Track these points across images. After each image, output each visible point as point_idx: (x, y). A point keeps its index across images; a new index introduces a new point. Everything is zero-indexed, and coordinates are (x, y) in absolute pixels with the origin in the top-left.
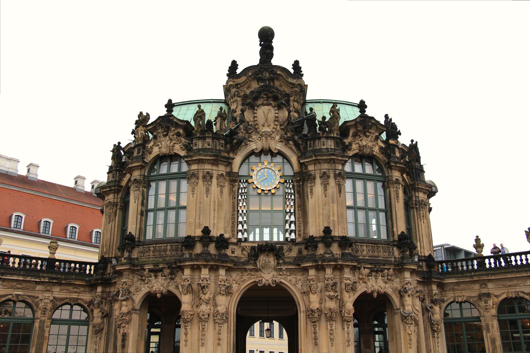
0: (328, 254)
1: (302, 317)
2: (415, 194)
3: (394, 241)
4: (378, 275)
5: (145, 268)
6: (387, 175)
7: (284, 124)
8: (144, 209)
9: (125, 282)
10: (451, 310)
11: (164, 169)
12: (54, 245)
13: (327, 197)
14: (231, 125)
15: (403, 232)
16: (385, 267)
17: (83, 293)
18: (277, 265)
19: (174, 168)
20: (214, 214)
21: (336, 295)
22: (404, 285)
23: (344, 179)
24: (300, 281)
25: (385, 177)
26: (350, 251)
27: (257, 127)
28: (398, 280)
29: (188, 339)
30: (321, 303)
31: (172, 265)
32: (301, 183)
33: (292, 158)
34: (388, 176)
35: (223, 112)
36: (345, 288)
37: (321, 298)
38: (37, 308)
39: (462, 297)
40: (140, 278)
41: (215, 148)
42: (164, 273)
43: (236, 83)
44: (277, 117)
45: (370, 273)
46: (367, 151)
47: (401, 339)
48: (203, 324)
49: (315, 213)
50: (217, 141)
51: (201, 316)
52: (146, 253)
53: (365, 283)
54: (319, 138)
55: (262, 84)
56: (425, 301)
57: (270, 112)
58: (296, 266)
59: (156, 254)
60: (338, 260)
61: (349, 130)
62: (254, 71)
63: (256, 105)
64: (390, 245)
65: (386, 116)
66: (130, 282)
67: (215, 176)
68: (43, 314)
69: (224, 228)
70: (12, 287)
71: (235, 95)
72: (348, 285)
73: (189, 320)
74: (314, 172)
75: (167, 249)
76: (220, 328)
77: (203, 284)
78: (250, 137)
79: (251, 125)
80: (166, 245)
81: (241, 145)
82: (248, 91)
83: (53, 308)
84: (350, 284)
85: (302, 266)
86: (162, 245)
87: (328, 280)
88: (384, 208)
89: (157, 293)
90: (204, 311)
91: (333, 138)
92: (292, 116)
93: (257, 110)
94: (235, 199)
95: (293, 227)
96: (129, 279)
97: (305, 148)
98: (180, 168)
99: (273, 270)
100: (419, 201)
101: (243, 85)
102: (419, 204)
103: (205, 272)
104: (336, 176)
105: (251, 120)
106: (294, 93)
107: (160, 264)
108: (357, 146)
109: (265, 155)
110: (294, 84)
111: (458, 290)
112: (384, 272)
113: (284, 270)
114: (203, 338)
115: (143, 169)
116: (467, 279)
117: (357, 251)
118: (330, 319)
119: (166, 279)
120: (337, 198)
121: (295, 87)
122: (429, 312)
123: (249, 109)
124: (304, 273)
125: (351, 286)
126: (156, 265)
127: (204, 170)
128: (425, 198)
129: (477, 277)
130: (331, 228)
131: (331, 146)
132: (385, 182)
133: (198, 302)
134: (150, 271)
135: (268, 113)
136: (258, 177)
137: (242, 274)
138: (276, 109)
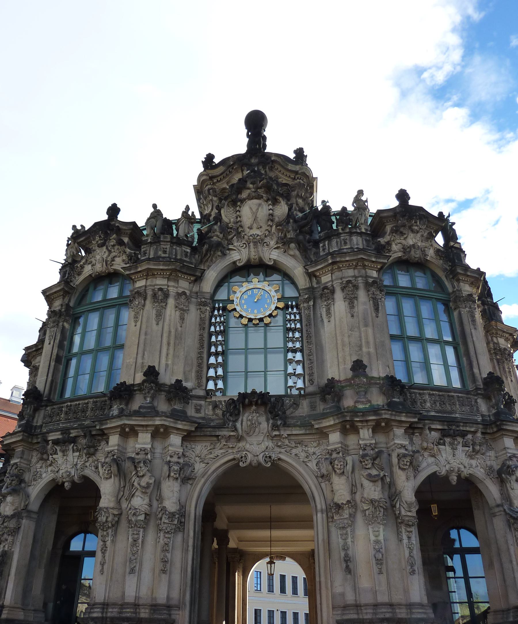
0: (362, 403)
3: (477, 389)
13: (355, 317)
15: (490, 374)
16: (468, 429)
18: (272, 429)
19: (114, 292)
20: (168, 349)
22: (506, 460)
23: (383, 293)
24: (315, 456)
26: (402, 400)
28: (492, 453)
29: (107, 561)
30: (353, 493)
31: (90, 431)
32: (311, 303)
41: (174, 257)
42: (77, 446)
43: (210, 175)
44: (272, 215)
45: (440, 439)
46: (416, 255)
47: (511, 562)
49: (337, 343)
50: (178, 248)
53: (433, 456)
54: (337, 234)
55: (248, 172)
57: (260, 208)
58: (306, 430)
59: (70, 417)
61: (385, 226)
64: (471, 394)
69: (184, 373)
75: (87, 407)
77: (138, 459)
78: (229, 244)
79: (231, 228)
80: (86, 401)
85: (316, 426)
86: (81, 402)
87: (365, 449)
90: (136, 507)
91: (361, 234)
93: (240, 207)
95: (299, 370)
97: (317, 254)
98: (121, 291)
99: (266, 439)
101: (221, 179)
104: (368, 285)
105: (232, 220)
107: (72, 431)
110: (296, 173)
112: (466, 437)
113: (286, 438)
114: (133, 558)
117: (414, 402)
120: (372, 319)
123: (228, 206)
127: (155, 287)
130: (365, 362)
131: (357, 244)
133: (128, 492)
135: (258, 209)
136: (243, 301)
137: (212, 446)
138: (270, 203)
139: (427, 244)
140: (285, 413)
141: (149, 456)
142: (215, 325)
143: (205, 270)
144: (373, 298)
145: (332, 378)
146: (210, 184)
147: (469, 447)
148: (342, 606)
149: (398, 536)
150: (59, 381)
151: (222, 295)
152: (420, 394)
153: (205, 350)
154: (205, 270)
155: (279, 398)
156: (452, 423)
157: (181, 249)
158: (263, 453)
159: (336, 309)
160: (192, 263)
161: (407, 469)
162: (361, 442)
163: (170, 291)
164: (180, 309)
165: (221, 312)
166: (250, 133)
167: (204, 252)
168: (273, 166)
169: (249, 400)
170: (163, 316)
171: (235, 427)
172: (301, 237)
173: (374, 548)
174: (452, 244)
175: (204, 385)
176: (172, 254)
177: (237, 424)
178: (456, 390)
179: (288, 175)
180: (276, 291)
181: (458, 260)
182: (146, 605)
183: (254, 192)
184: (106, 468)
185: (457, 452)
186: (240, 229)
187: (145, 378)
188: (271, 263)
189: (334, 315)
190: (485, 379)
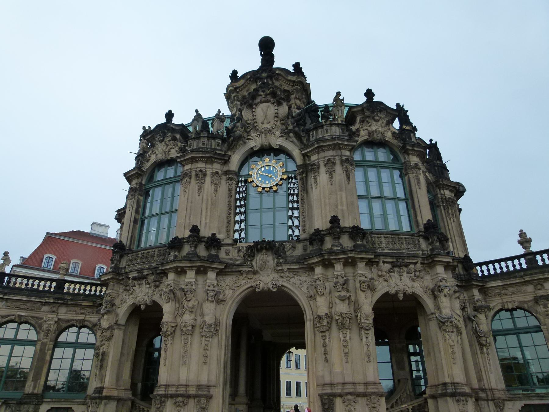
0: (336, 246)
1: (309, 326)
2: (440, 192)
3: (420, 232)
4: (402, 271)
5: (130, 276)
6: (403, 161)
8: (139, 217)
9: (109, 293)
10: (500, 319)
11: (160, 176)
12: (64, 266)
15: (429, 220)
16: (411, 261)
17: (91, 314)
18: (277, 265)
19: (170, 172)
20: (206, 212)
21: (348, 295)
22: (438, 282)
23: (353, 166)
24: (305, 284)
25: (402, 164)
26: (365, 243)
27: (256, 124)
28: (428, 277)
31: (156, 271)
32: (304, 175)
34: (405, 162)
36: (360, 287)
37: (331, 302)
38: (40, 329)
39: (513, 303)
40: (124, 287)
41: (210, 147)
42: (147, 281)
43: (234, 87)
44: (277, 113)
45: (391, 269)
46: (377, 137)
47: (440, 352)
48: (186, 338)
50: (213, 141)
51: (182, 327)
52: (134, 261)
53: (386, 281)
54: (322, 126)
56: (466, 309)
58: (300, 265)
60: (349, 252)
64: (415, 236)
65: (398, 105)
66: (116, 293)
67: (209, 173)
68: (45, 336)
69: (218, 228)
70: (16, 308)
71: (234, 100)
72: (364, 282)
73: (169, 333)
74: (317, 161)
76: (206, 343)
77: (187, 289)
78: (248, 135)
79: (249, 124)
80: (154, 250)
81: (239, 144)
83: (58, 330)
84: (366, 281)
86: (150, 251)
87: (337, 278)
88: (404, 197)
89: (140, 304)
90: (186, 321)
91: (338, 125)
93: (255, 109)
94: (231, 197)
96: (113, 289)
97: (308, 140)
98: (176, 172)
99: (273, 272)
100: (446, 199)
101: (242, 89)
102: (447, 202)
103: (191, 275)
104: (342, 162)
105: (250, 118)
107: (144, 271)
108: (366, 132)
111: (506, 294)
112: (409, 267)
113: (286, 271)
114: (184, 355)
115: (140, 178)
116: (516, 280)
117: (374, 243)
118: (342, 326)
119: (150, 288)
122: (472, 323)
123: (247, 108)
124: (310, 273)
125: (368, 283)
126: (140, 272)
128: (452, 197)
129: (529, 276)
130: (339, 218)
131: (335, 132)
132: (403, 169)
133: (181, 311)
134: (134, 279)
135: (267, 109)
136: (259, 175)
138: (275, 104)
139: (386, 129)
140: (286, 254)
141: (194, 287)
142: (239, 193)
143: (231, 155)
144: (346, 171)
145: (317, 229)
147: (412, 273)
148: (322, 384)
149: (360, 337)
150: (137, 235)
151: (244, 171)
152: (378, 237)
153: (232, 212)
154: (231, 155)
155: (282, 243)
156: (400, 257)
158: (271, 282)
159: (320, 179)
161: (366, 291)
162: (335, 273)
163: (207, 171)
164: (214, 184)
165: (243, 184)
166: (262, 53)
167: (231, 142)
169: (260, 246)
170: (203, 189)
171: (252, 264)
172: (297, 129)
173: (343, 345)
174: (404, 127)
175: (232, 236)
176: (208, 145)
177: (253, 262)
178: (404, 234)
179: (289, 83)
180: (281, 167)
181: (409, 139)
182: (193, 386)
183: (265, 97)
184: (166, 295)
185: (402, 278)
187: (191, 233)
188: (277, 147)
189: (320, 184)
190: (425, 225)
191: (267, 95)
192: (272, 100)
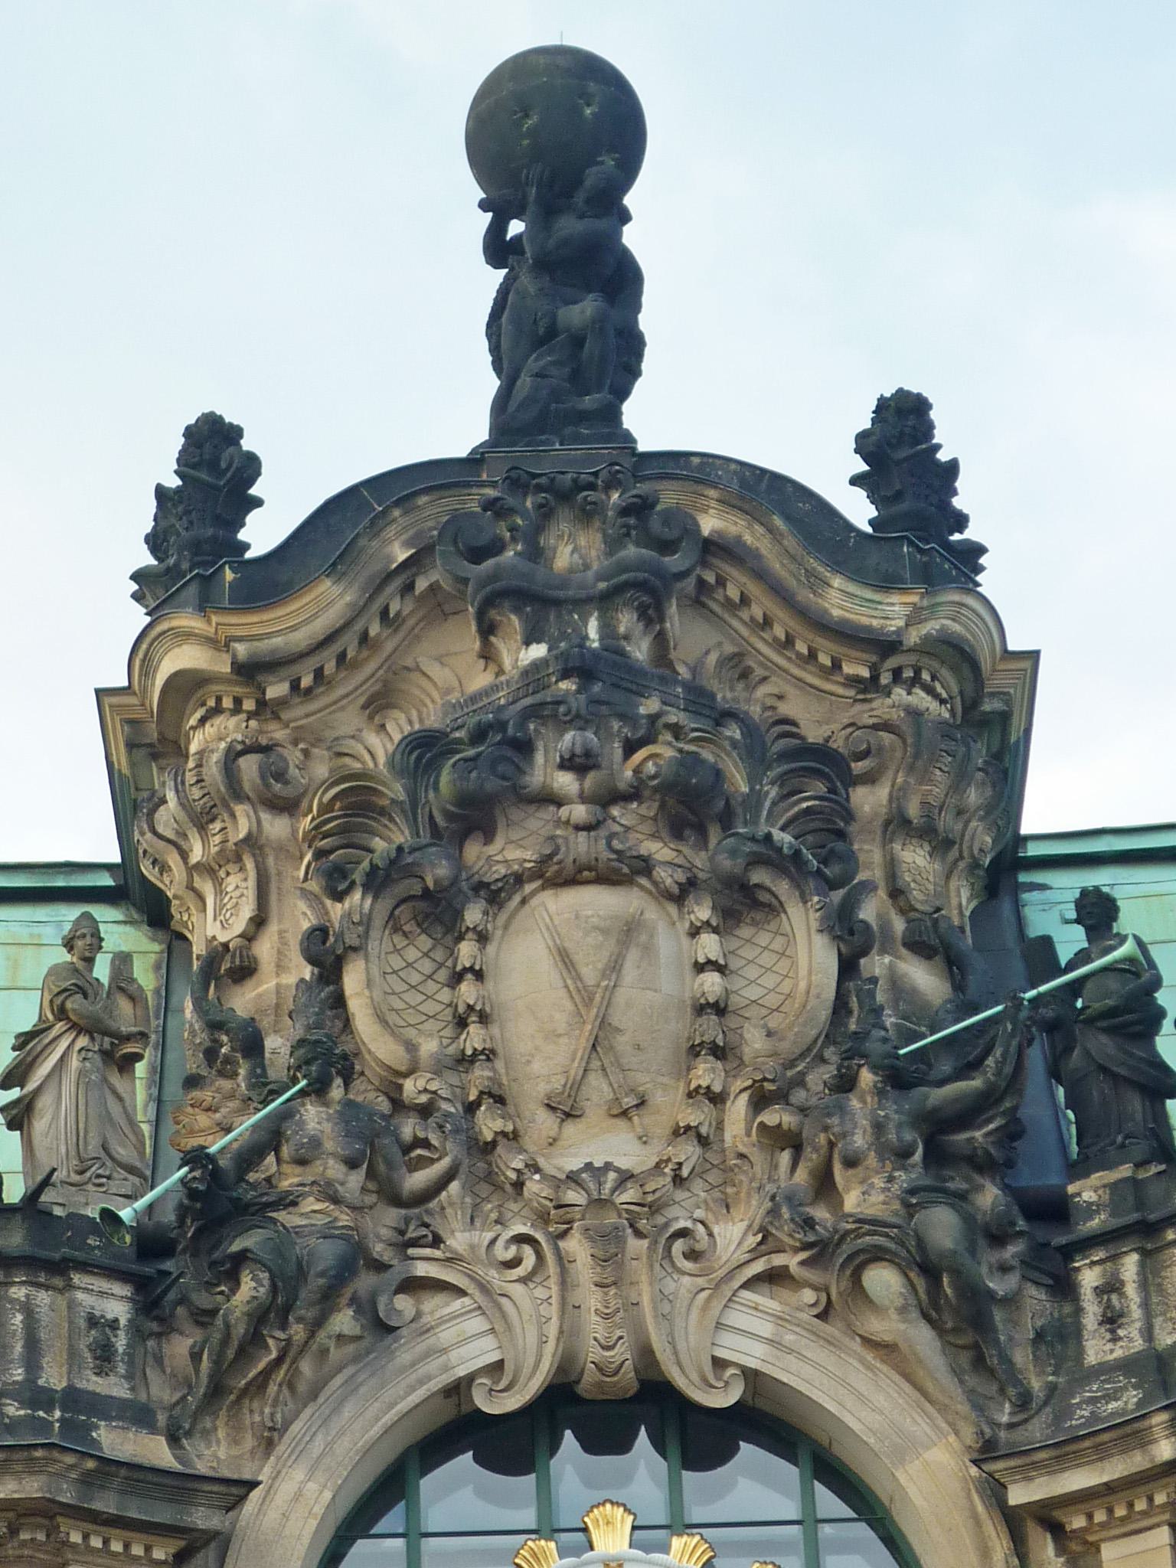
7: (800, 1081)
14: (203, 1120)
33: (914, 1467)
35: (102, 970)
41: (18, 1374)
43: (241, 649)
44: (719, 1009)
57: (632, 956)
62: (432, 512)
63: (480, 887)
78: (415, 1243)
79: (425, 1111)
81: (321, 1336)
82: (374, 740)
92: (880, 997)
93: (483, 938)
101: (319, 673)
105: (429, 1047)
106: (886, 737)
109: (592, 1445)
110: (885, 646)
121: (897, 673)
123: (394, 924)
135: (615, 967)
138: (703, 912)
146: (238, 701)
157: (61, 1302)
160: (140, 1416)
167: (240, 1330)
168: (710, 578)
179: (825, 660)
183: (588, 828)
186: (488, 1124)
191: (608, 798)
192: (659, 850)
